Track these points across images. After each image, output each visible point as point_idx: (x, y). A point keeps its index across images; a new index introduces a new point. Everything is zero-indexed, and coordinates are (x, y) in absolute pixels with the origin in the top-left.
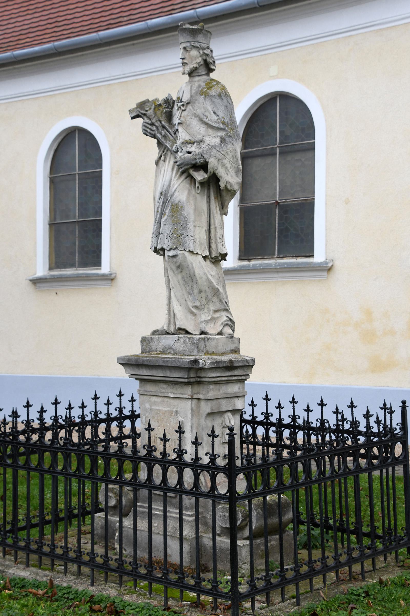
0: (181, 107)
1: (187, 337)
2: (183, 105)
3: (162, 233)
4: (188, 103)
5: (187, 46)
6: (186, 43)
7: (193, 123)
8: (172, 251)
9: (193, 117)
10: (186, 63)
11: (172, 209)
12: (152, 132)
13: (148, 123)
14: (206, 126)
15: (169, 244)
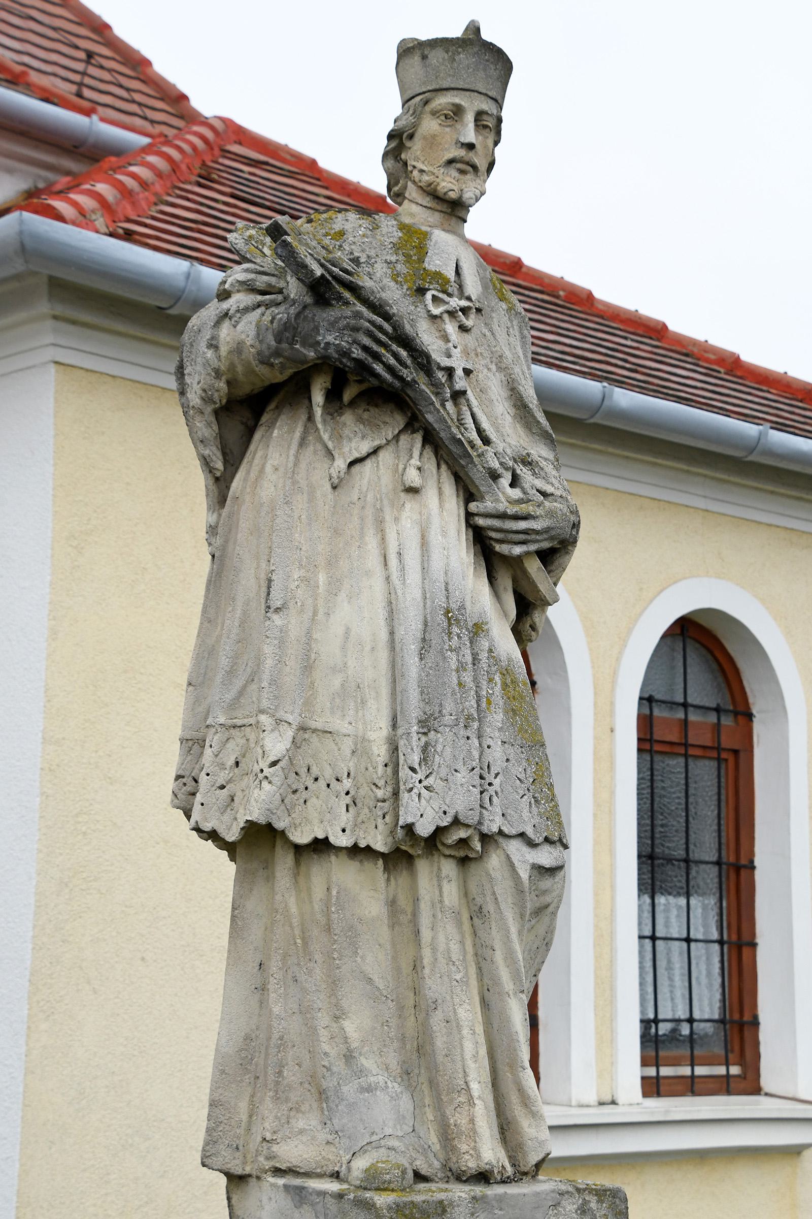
0: (460, 313)
1: (589, 1190)
2: (465, 310)
3: (497, 775)
4: (479, 310)
5: (491, 115)
6: (490, 102)
7: (493, 388)
8: (547, 847)
9: (493, 367)
10: (475, 168)
11: (505, 686)
12: (404, 372)
13: (380, 328)
14: (512, 411)
15: (537, 820)
